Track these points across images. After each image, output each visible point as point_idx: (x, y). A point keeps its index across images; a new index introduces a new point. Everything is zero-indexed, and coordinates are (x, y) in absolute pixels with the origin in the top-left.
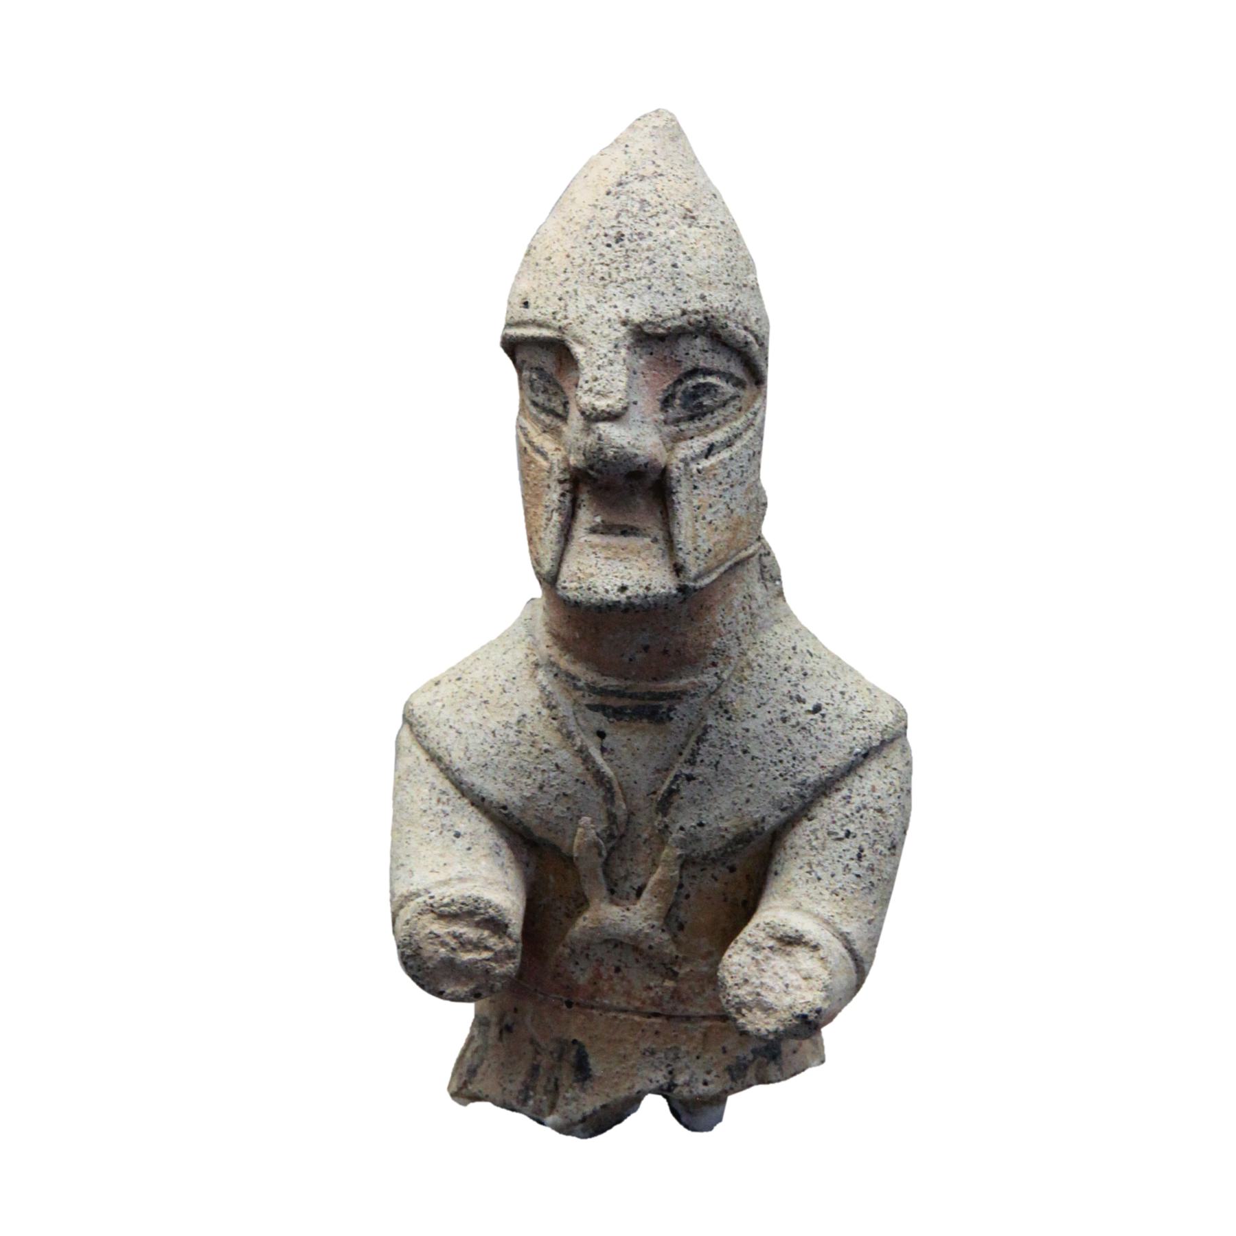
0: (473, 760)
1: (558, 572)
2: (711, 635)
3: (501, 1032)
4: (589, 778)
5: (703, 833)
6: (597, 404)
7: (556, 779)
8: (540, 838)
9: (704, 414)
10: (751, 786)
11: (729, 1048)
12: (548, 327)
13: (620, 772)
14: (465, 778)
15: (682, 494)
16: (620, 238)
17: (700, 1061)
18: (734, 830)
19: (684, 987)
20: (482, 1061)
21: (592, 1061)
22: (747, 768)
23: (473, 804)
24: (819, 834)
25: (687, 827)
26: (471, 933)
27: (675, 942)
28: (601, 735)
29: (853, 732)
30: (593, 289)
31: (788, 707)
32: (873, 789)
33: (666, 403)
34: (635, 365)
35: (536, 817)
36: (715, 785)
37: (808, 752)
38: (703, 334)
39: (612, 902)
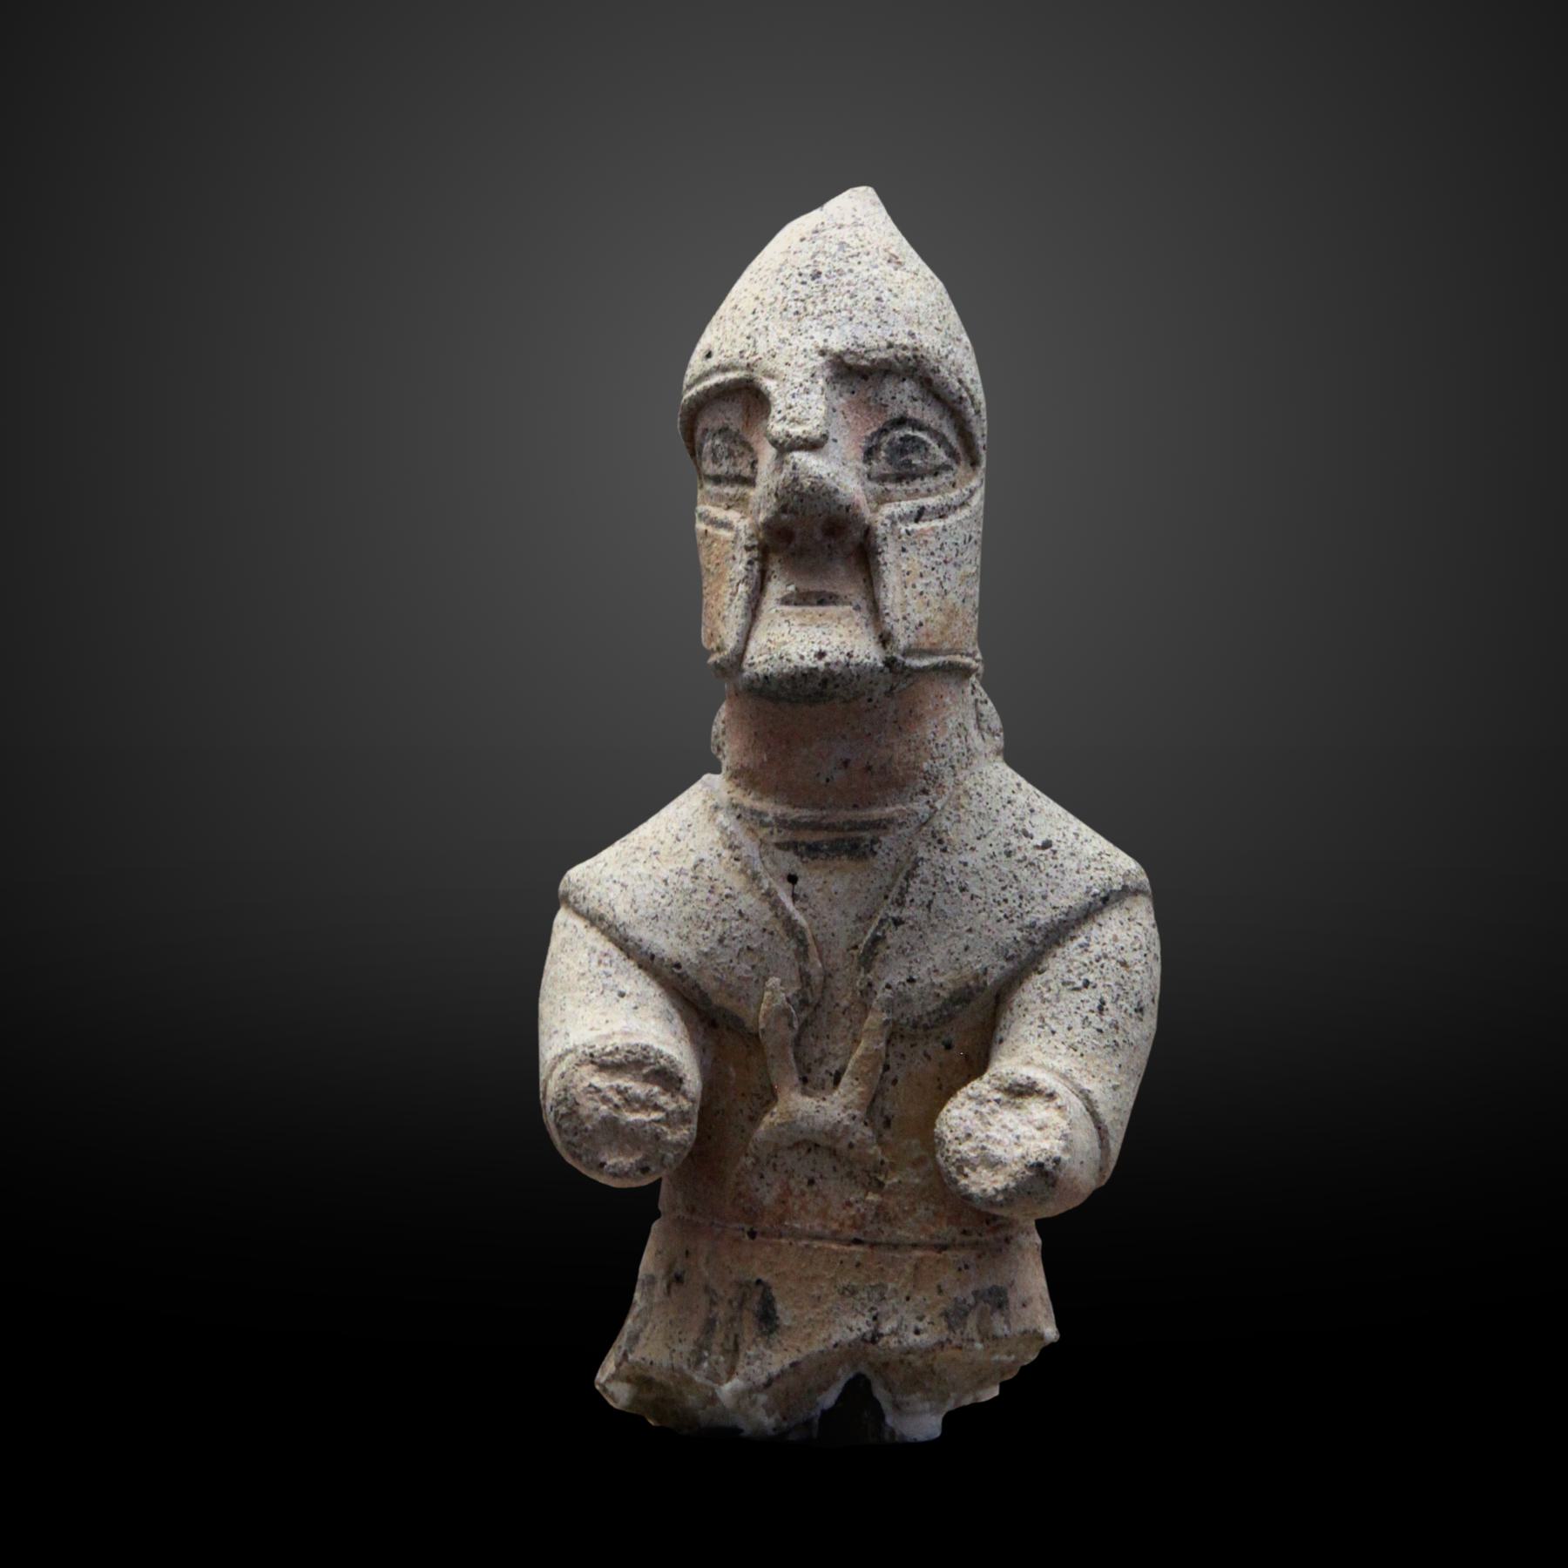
0: (641, 912)
1: (745, 650)
2: (922, 752)
3: (669, 1287)
4: (778, 927)
5: (913, 992)
6: (791, 431)
7: (740, 929)
8: (719, 1008)
9: (914, 477)
10: (970, 930)
11: (946, 1287)
12: (735, 368)
13: (815, 922)
14: (631, 933)
15: (889, 554)
16: (816, 275)
17: (911, 1303)
18: (950, 986)
19: (891, 1202)
20: (646, 1324)
21: (779, 1307)
22: (965, 910)
23: (640, 967)
24: (1052, 985)
25: (895, 983)
26: (638, 1089)
27: (880, 1143)
28: (792, 879)
29: (1091, 872)
30: (786, 323)
31: (1014, 840)
32: (1115, 939)
33: (869, 454)
34: (835, 403)
35: (716, 979)
36: (928, 931)
37: (1037, 891)
38: (912, 377)
39: (805, 1093)
